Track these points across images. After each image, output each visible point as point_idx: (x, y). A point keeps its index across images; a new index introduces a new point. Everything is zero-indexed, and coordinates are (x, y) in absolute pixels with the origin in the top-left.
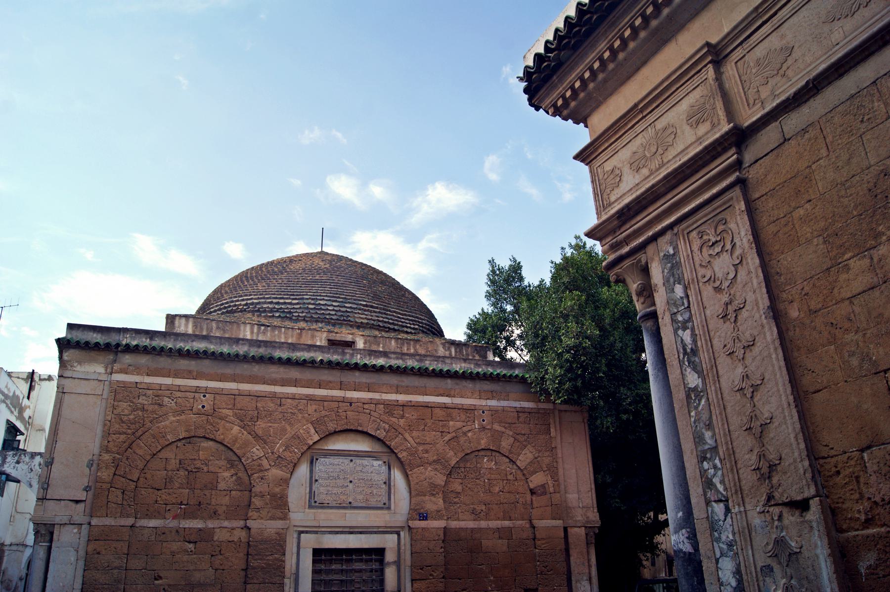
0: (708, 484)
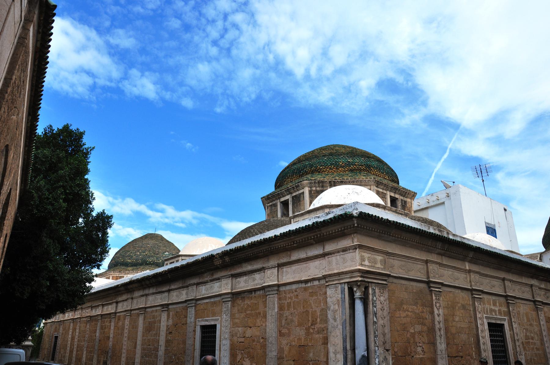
0: (375, 343)
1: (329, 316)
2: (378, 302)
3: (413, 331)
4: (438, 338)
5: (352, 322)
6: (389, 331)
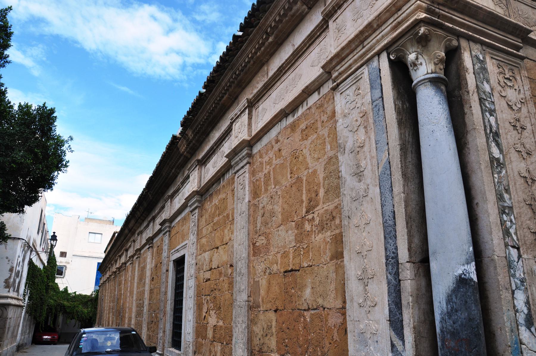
0: (506, 233)
1: (343, 169)
2: (500, 105)
5: (411, 168)
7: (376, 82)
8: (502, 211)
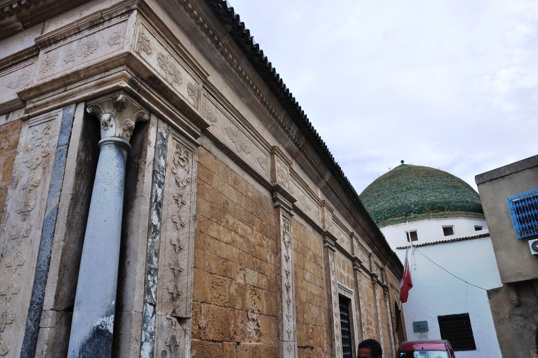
0: (148, 291)
1: (9, 203)
2: (169, 180)
3: (242, 282)
4: (285, 305)
5: (78, 218)
6: (191, 265)
7: (66, 128)
8: (148, 272)
